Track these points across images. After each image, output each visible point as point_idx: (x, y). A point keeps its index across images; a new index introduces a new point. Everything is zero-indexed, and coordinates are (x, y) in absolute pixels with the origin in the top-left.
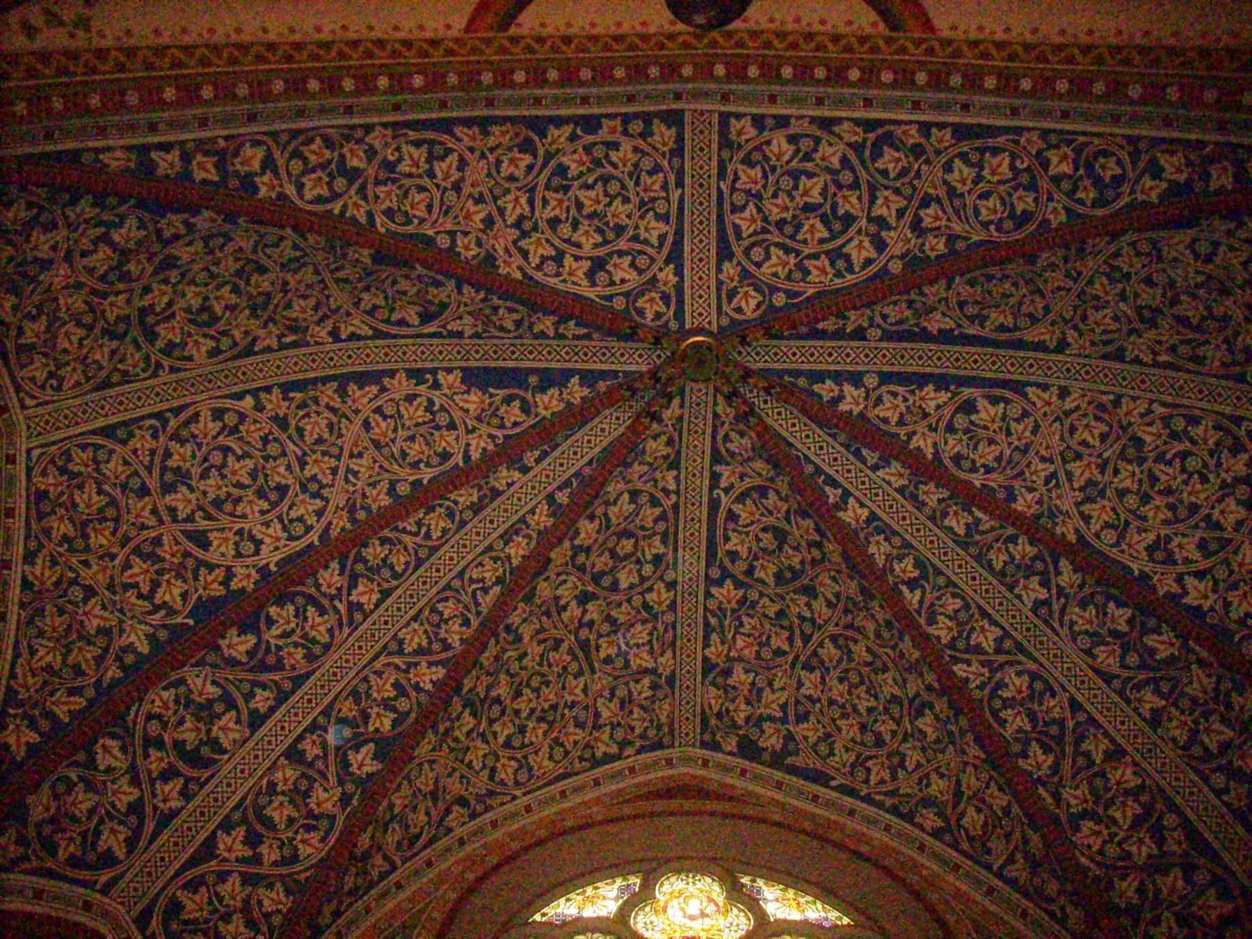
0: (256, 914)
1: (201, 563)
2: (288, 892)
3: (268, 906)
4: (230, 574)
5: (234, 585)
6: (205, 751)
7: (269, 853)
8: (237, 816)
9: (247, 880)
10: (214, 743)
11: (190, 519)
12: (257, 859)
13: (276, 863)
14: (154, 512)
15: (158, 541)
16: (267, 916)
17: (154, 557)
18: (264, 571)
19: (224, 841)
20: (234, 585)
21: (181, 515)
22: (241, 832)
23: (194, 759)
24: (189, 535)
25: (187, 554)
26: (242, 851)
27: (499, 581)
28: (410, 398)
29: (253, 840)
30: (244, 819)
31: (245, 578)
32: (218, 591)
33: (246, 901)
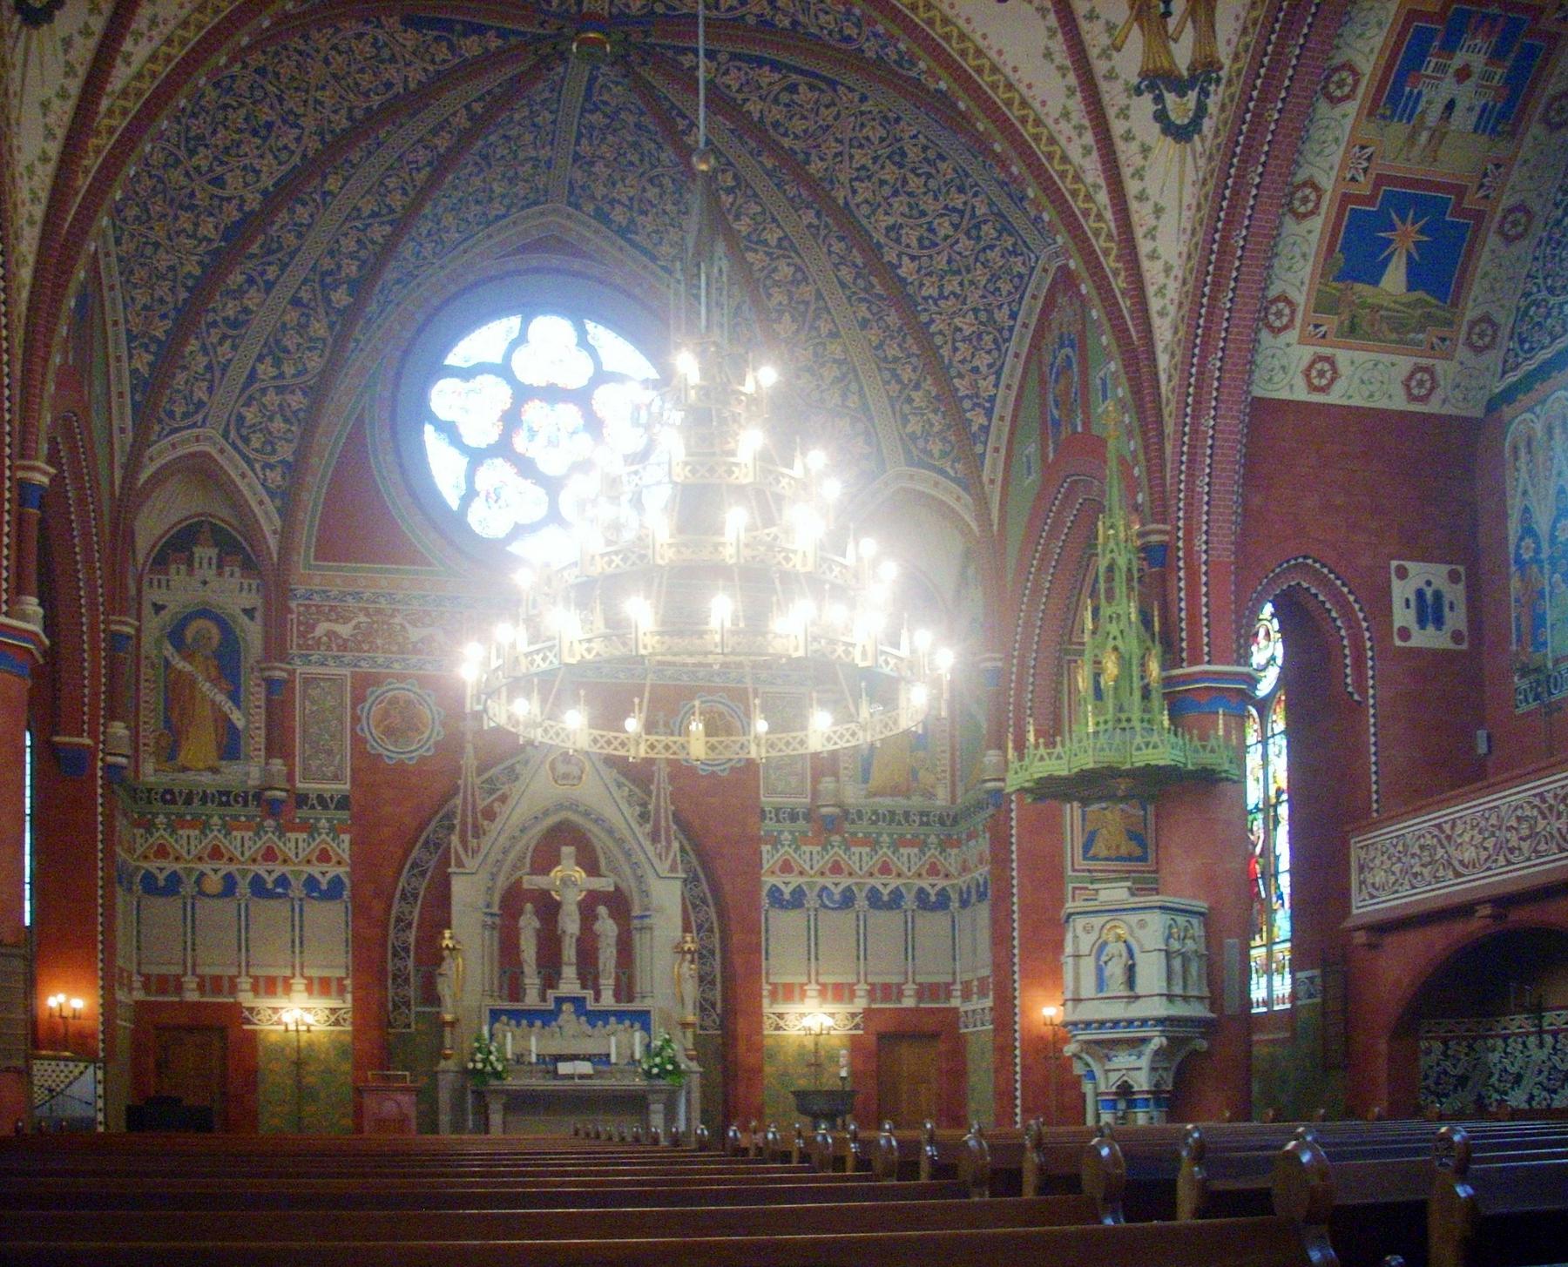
0: (288, 414)
1: (222, 199)
2: (305, 394)
3: (295, 406)
4: (243, 200)
5: (246, 208)
6: (242, 317)
7: (289, 370)
8: (265, 351)
9: (280, 390)
10: (246, 310)
11: (211, 170)
12: (281, 376)
13: (293, 376)
14: (187, 174)
15: (192, 195)
16: (295, 413)
17: (192, 207)
18: (265, 192)
19: (261, 368)
20: (246, 208)
21: (204, 169)
22: (269, 360)
23: (234, 324)
24: (212, 182)
25: (212, 197)
26: (273, 372)
27: (430, 163)
28: (360, 36)
29: (277, 363)
30: (271, 352)
31: (254, 202)
32: (236, 216)
33: (280, 405)
